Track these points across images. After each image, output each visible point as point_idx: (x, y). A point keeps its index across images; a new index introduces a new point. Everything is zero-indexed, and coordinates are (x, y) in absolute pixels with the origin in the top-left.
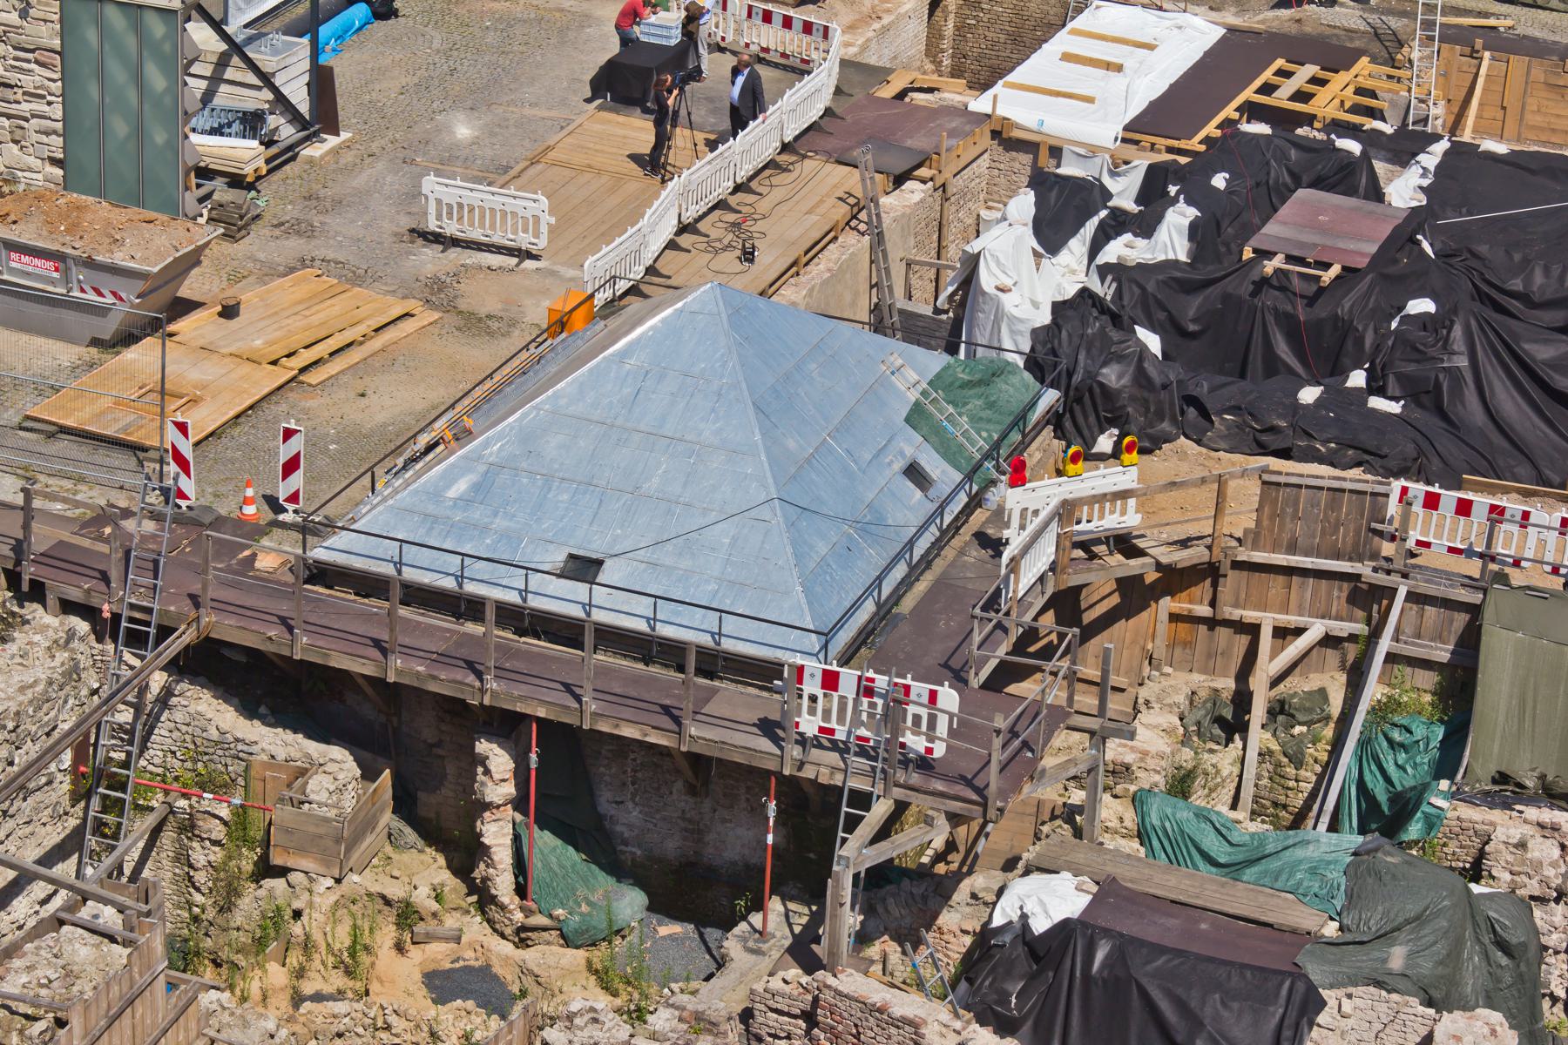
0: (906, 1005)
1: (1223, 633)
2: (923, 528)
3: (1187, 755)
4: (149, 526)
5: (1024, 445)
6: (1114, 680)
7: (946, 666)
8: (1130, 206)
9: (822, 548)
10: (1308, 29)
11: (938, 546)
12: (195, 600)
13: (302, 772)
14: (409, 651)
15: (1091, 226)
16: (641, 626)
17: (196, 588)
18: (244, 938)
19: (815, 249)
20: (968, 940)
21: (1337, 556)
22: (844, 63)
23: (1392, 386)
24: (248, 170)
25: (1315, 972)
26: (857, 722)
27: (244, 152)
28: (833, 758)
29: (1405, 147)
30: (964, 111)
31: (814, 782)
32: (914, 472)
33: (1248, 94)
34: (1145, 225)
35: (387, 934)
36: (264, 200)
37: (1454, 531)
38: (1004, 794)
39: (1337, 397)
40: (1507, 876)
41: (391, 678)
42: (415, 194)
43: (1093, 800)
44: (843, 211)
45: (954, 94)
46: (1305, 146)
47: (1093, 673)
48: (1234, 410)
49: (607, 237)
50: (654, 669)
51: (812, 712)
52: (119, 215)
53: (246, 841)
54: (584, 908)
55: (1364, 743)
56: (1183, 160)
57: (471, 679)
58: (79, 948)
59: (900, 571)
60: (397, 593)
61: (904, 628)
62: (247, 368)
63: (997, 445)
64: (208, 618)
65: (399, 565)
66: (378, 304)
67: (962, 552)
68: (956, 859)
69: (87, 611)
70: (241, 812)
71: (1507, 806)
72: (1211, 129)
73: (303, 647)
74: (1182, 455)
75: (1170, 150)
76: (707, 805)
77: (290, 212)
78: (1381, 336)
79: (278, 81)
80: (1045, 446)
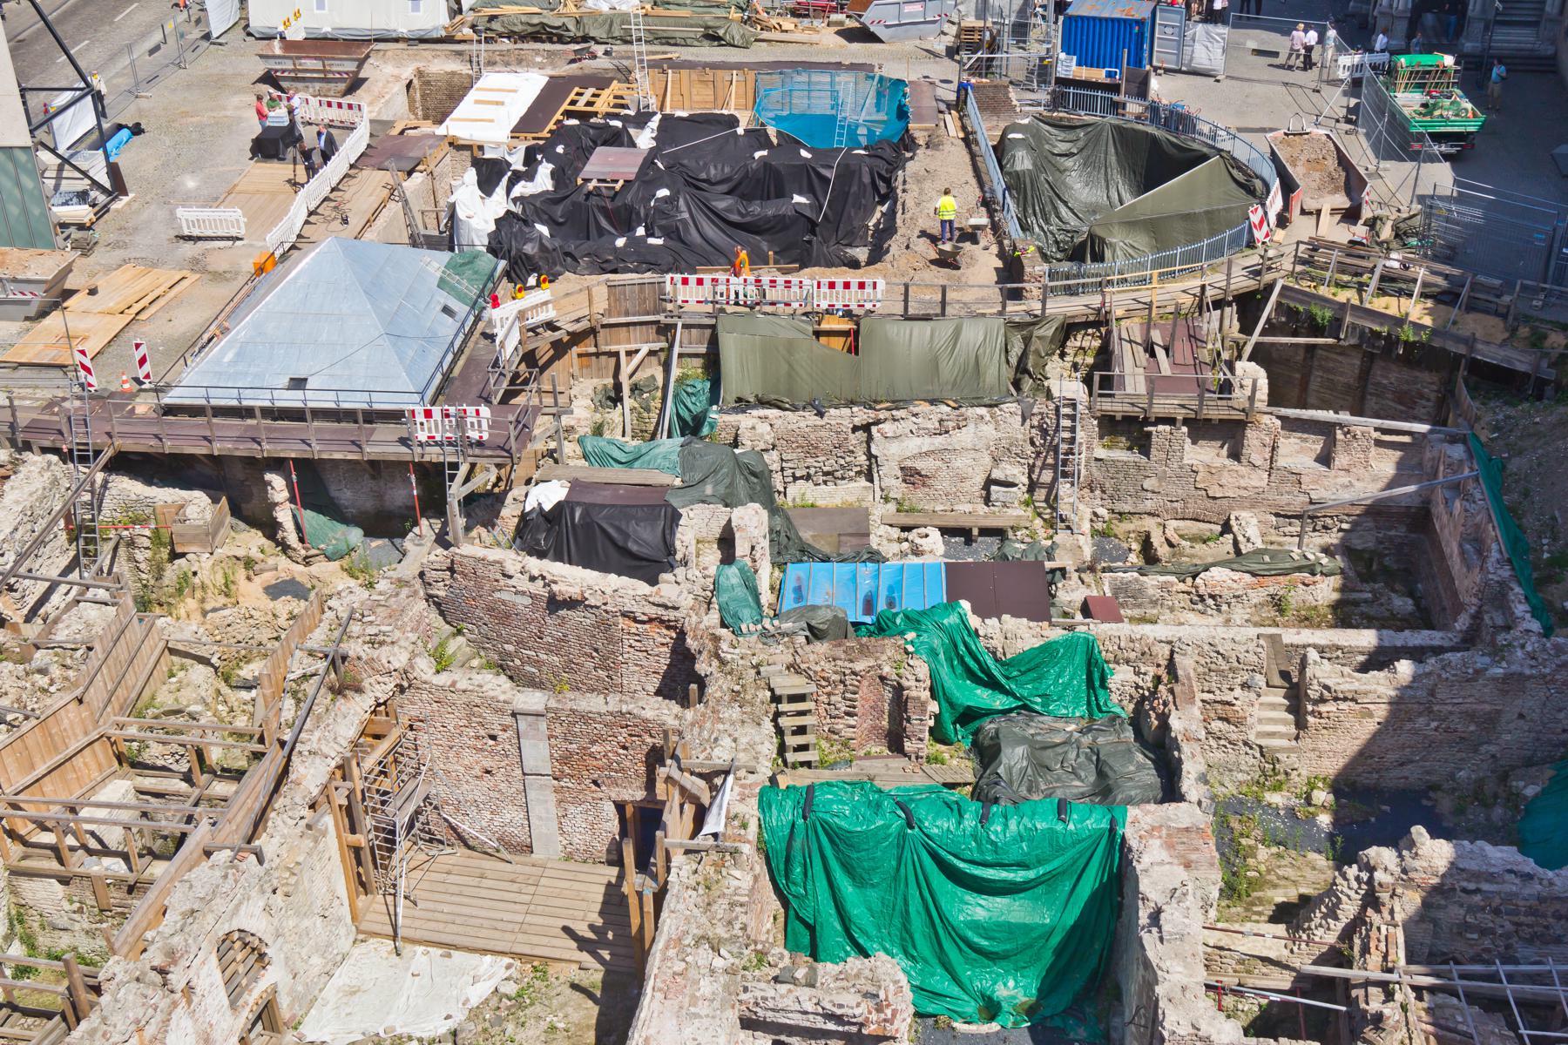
0: (494, 554)
1: (603, 358)
2: (456, 335)
3: (598, 416)
4: (77, 403)
5: (495, 288)
6: (559, 389)
7: (480, 397)
8: (523, 169)
9: (411, 353)
10: (586, 72)
11: (465, 342)
12: (109, 435)
13: (182, 506)
14: (222, 439)
15: (505, 180)
16: (333, 405)
17: (108, 429)
18: (171, 590)
19: (376, 213)
20: (516, 520)
21: (648, 314)
22: (372, 121)
23: (657, 232)
24: (86, 220)
25: (675, 502)
26: (445, 431)
27: (82, 212)
28: (437, 449)
29: (642, 119)
30: (434, 136)
31: (430, 462)
32: (447, 310)
33: (565, 106)
34: (530, 176)
35: (241, 574)
36: (98, 233)
37: (697, 292)
38: (519, 451)
39: (634, 242)
40: (749, 443)
41: (216, 453)
42: (173, 216)
43: (560, 444)
44: (386, 192)
45: (427, 128)
46: (594, 127)
47: (547, 387)
48: (588, 255)
49: (274, 223)
50: (343, 425)
51: (423, 430)
52: (25, 254)
53: (162, 544)
54: (334, 542)
55: (676, 396)
56: (541, 142)
57: (256, 446)
58: (90, 612)
59: (450, 357)
60: (210, 412)
61: (457, 383)
62: (109, 318)
63: (482, 291)
64: (118, 442)
65: (207, 399)
66: (167, 276)
67: (476, 343)
68: (502, 484)
69: (55, 451)
70: (156, 531)
71: (744, 412)
72: (551, 126)
73: (169, 446)
74: (568, 280)
75: (534, 139)
76: (382, 483)
77: (112, 237)
78: (647, 209)
79: (91, 174)
80: (505, 287)
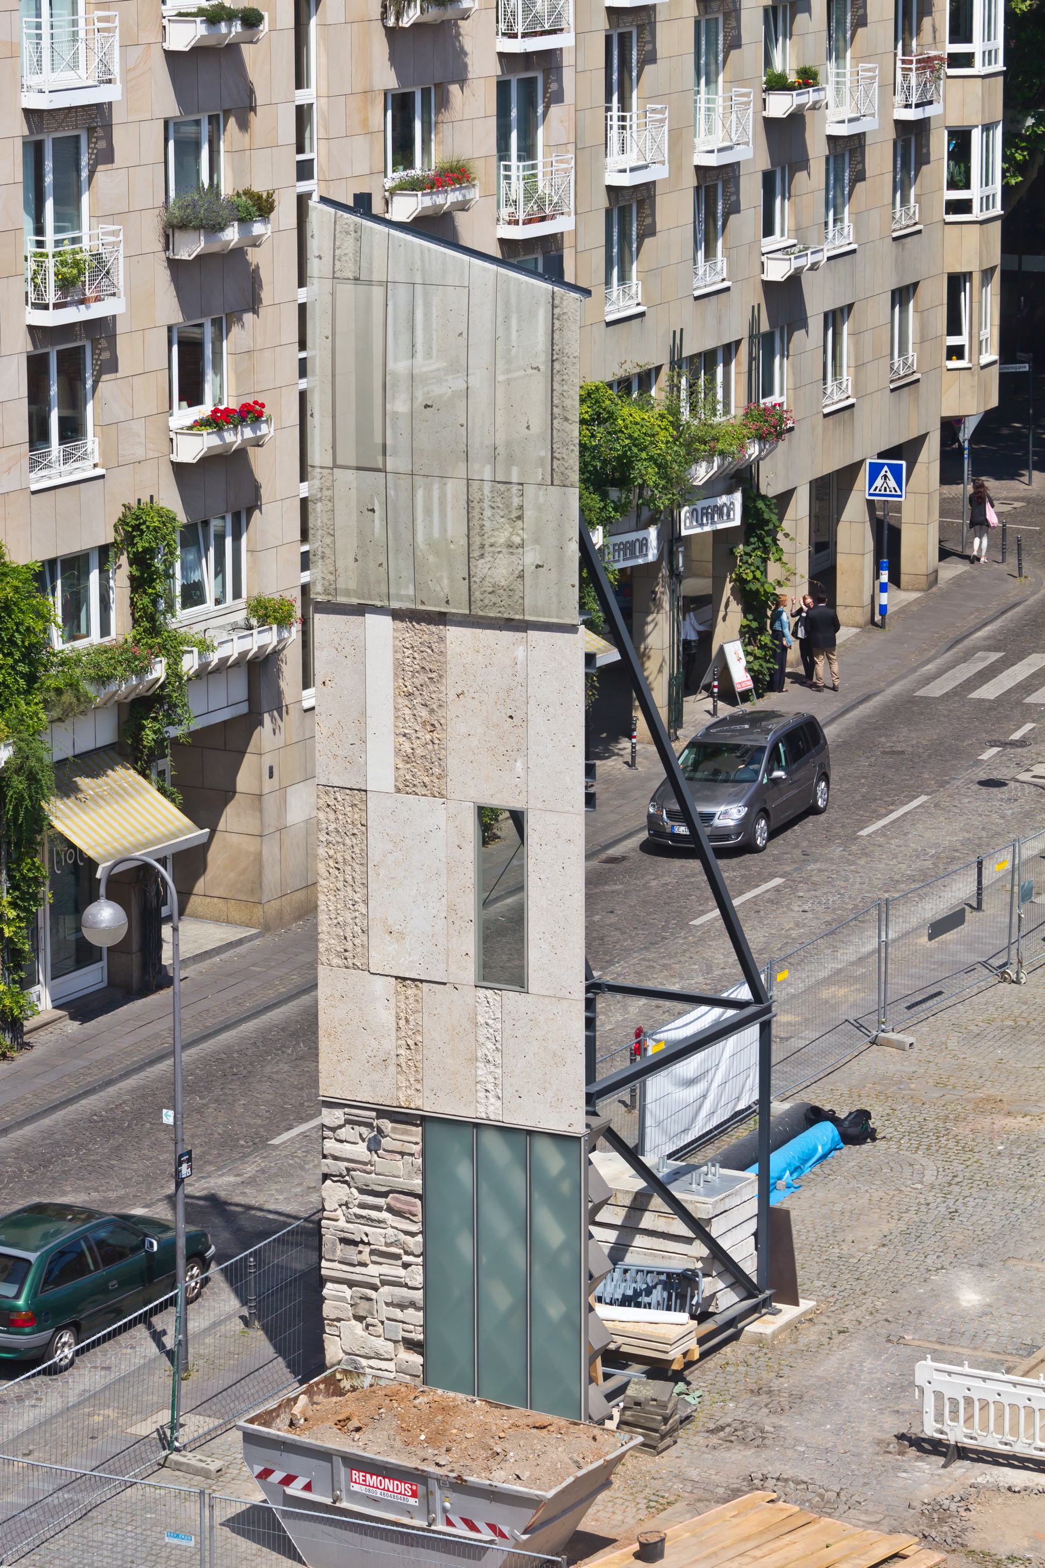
24: (675, 1353)
42: (906, 1385)
52: (499, 1419)
77: (732, 1411)
79: (715, 1230)
